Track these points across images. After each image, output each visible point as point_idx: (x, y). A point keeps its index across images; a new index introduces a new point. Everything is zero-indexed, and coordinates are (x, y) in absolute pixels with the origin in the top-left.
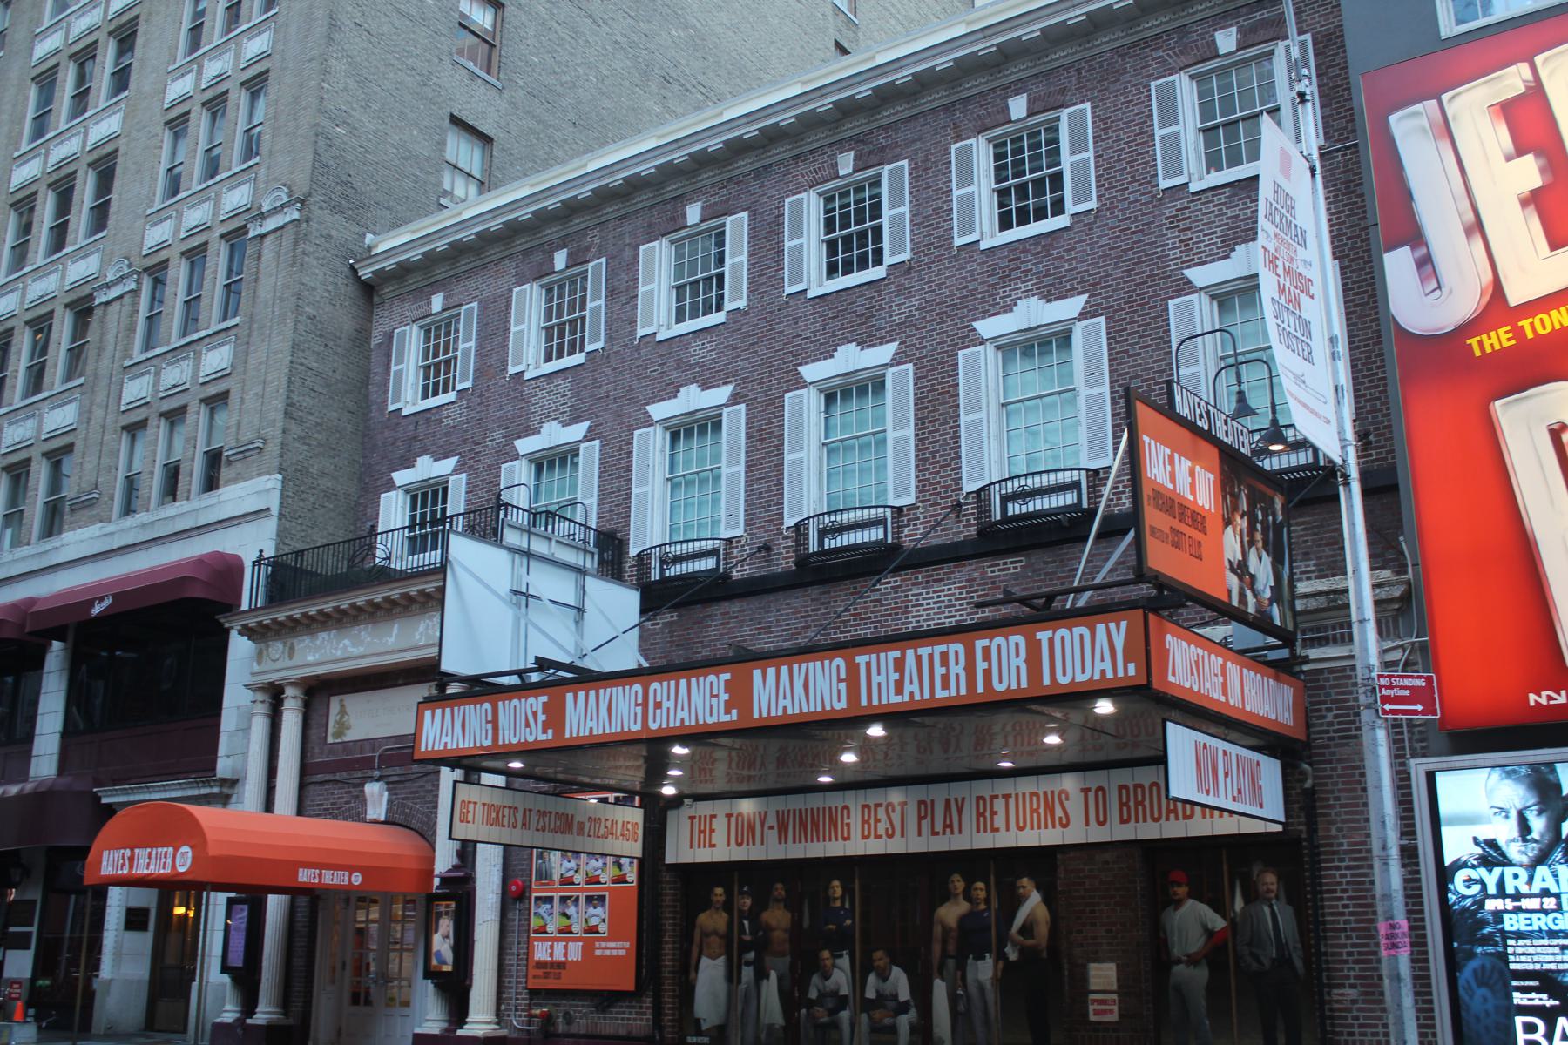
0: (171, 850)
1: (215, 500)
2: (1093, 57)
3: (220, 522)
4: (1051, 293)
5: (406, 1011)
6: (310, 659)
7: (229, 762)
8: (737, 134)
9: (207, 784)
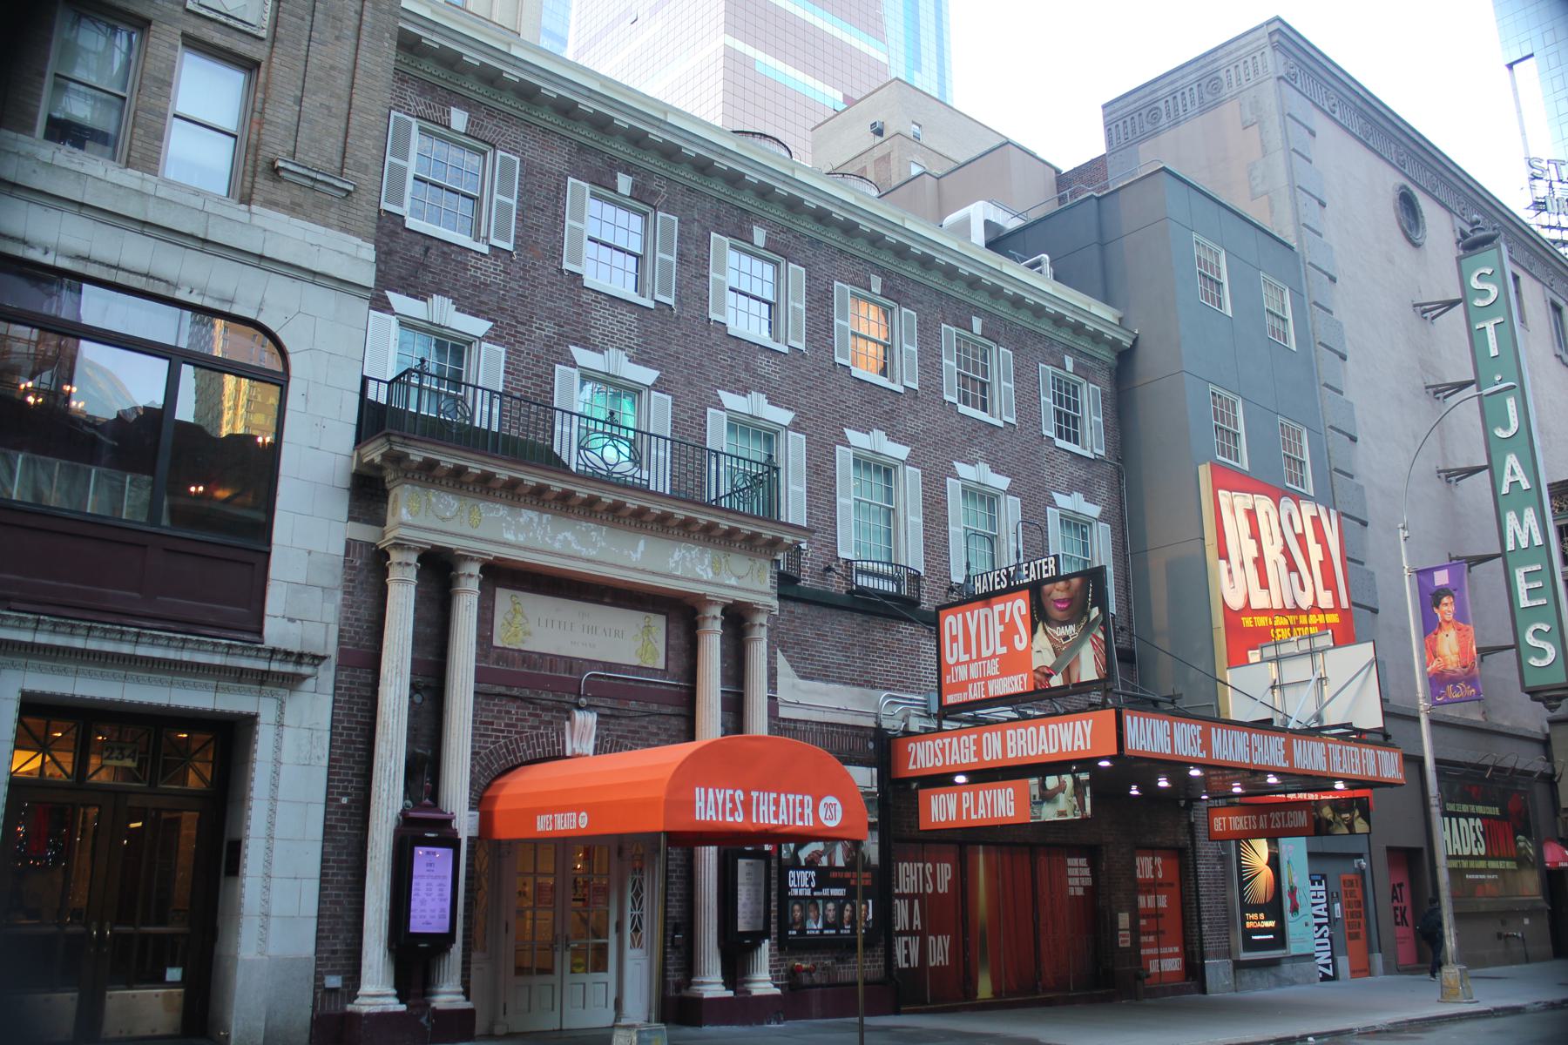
0: (808, 798)
2: (1012, 323)
3: (261, 257)
5: (601, 976)
6: (509, 536)
7: (295, 628)
9: (244, 652)
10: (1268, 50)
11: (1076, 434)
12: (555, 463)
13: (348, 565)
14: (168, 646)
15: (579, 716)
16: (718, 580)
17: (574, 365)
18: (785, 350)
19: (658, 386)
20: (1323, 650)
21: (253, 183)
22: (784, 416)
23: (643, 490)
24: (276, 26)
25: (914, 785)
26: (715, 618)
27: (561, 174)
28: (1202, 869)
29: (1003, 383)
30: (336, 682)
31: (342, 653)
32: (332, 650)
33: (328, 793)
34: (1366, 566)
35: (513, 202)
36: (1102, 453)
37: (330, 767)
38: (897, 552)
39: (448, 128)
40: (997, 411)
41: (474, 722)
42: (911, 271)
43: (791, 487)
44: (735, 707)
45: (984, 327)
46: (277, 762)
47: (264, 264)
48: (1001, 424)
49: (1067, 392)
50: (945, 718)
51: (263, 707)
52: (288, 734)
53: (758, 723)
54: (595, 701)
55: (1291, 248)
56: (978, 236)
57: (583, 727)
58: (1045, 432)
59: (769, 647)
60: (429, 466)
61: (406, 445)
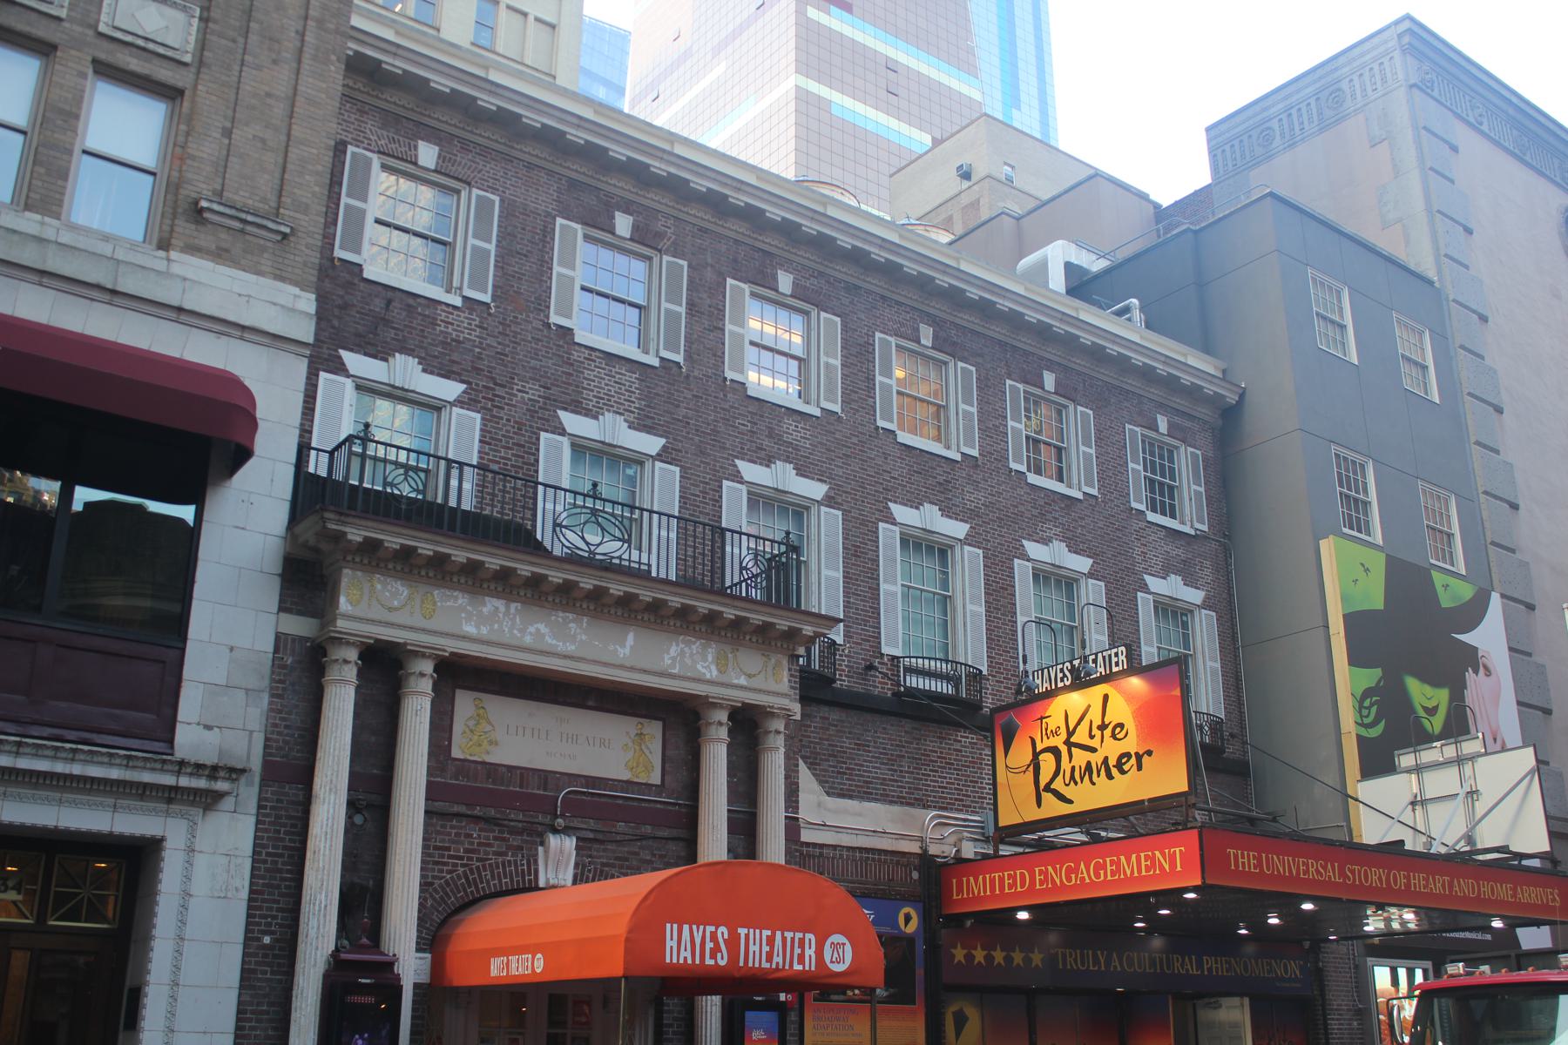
0: (809, 936)
1: (161, 265)
2: (1092, 378)
3: (180, 310)
4: (1074, 549)
6: (470, 629)
7: (213, 737)
8: (867, 247)
9: (146, 764)
10: (1397, 54)
11: (1172, 507)
12: (538, 549)
13: (277, 663)
14: (55, 758)
15: (554, 841)
16: (724, 679)
17: (563, 432)
18: (817, 413)
19: (664, 456)
20: (1472, 758)
21: (172, 226)
22: (815, 490)
23: (643, 575)
24: (203, 49)
25: (968, 923)
26: (720, 724)
27: (548, 214)
28: (1334, 1025)
29: (1082, 448)
30: (260, 799)
31: (267, 765)
32: (256, 764)
33: (247, 931)
34: (1535, 658)
35: (492, 247)
36: (1205, 528)
37: (250, 900)
38: (955, 647)
39: (415, 164)
40: (1075, 481)
41: (425, 847)
42: (966, 319)
43: (824, 572)
44: (744, 829)
45: (1058, 383)
46: (187, 894)
47: (183, 318)
48: (1080, 496)
49: (1161, 457)
50: (1003, 842)
51: (169, 828)
52: (201, 861)
53: (774, 848)
54: (576, 823)
55: (1430, 283)
56: (1057, 281)
57: (559, 855)
58: (1134, 505)
59: (787, 757)
60: (371, 546)
61: (344, 523)
